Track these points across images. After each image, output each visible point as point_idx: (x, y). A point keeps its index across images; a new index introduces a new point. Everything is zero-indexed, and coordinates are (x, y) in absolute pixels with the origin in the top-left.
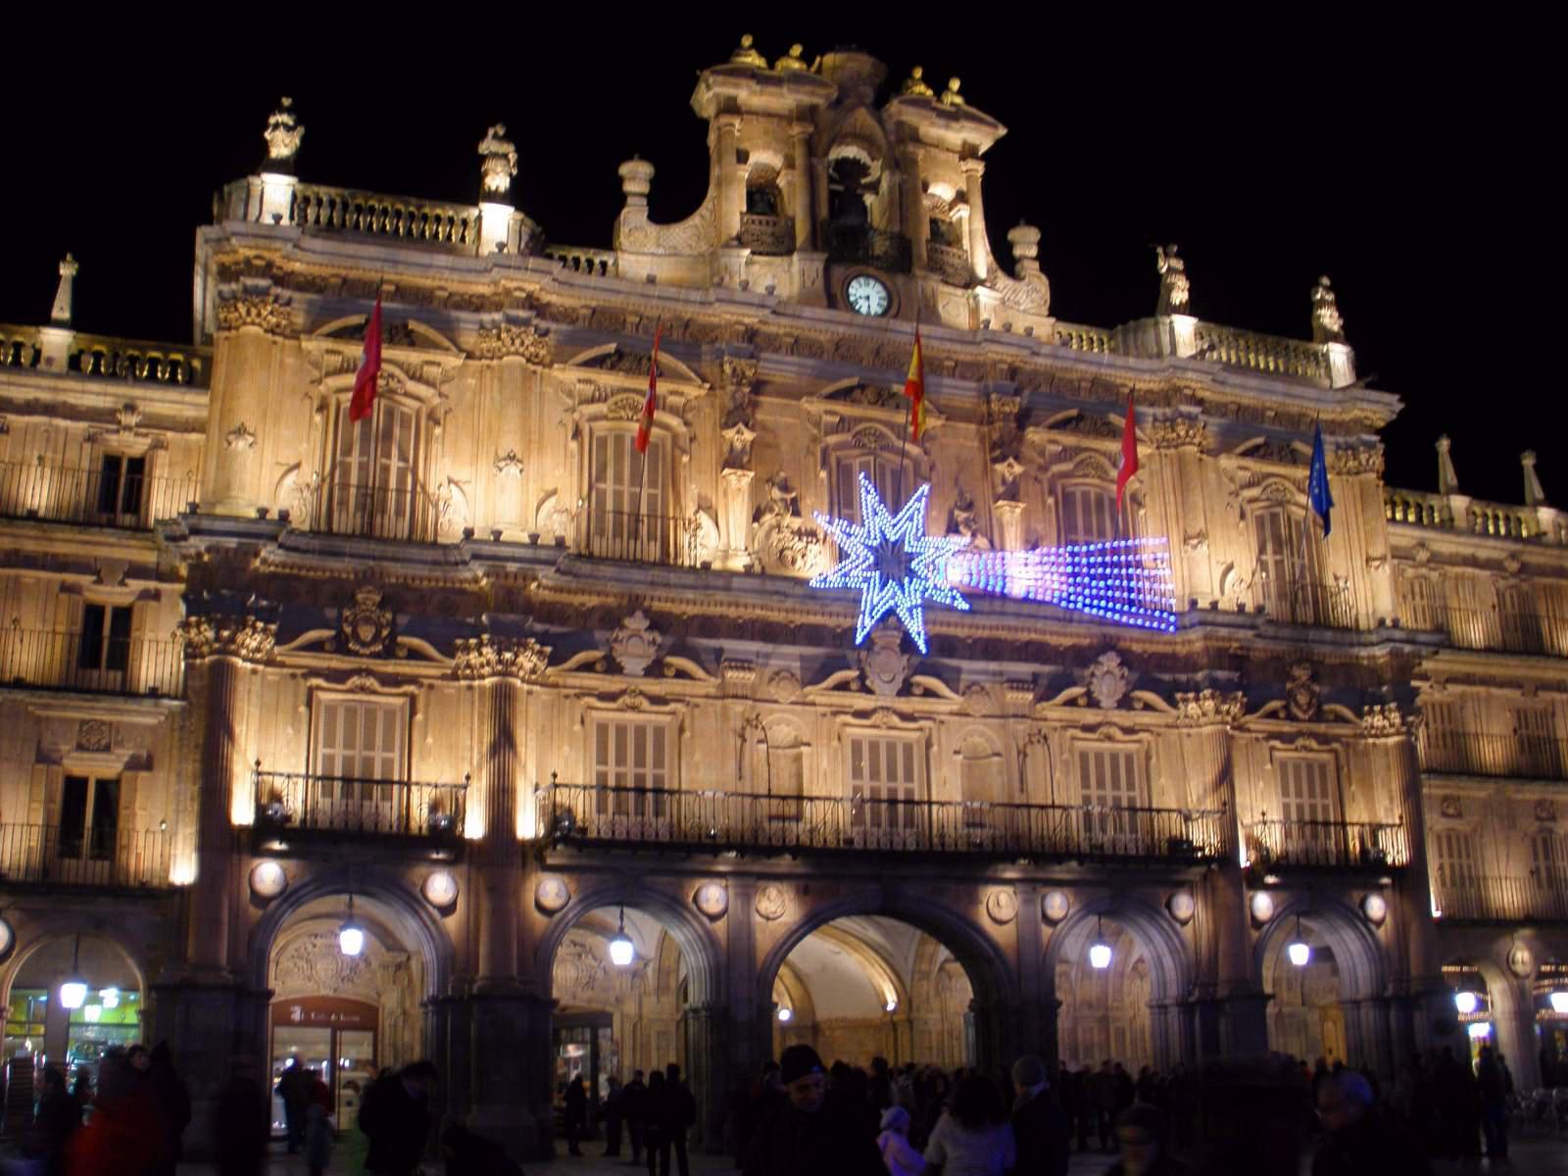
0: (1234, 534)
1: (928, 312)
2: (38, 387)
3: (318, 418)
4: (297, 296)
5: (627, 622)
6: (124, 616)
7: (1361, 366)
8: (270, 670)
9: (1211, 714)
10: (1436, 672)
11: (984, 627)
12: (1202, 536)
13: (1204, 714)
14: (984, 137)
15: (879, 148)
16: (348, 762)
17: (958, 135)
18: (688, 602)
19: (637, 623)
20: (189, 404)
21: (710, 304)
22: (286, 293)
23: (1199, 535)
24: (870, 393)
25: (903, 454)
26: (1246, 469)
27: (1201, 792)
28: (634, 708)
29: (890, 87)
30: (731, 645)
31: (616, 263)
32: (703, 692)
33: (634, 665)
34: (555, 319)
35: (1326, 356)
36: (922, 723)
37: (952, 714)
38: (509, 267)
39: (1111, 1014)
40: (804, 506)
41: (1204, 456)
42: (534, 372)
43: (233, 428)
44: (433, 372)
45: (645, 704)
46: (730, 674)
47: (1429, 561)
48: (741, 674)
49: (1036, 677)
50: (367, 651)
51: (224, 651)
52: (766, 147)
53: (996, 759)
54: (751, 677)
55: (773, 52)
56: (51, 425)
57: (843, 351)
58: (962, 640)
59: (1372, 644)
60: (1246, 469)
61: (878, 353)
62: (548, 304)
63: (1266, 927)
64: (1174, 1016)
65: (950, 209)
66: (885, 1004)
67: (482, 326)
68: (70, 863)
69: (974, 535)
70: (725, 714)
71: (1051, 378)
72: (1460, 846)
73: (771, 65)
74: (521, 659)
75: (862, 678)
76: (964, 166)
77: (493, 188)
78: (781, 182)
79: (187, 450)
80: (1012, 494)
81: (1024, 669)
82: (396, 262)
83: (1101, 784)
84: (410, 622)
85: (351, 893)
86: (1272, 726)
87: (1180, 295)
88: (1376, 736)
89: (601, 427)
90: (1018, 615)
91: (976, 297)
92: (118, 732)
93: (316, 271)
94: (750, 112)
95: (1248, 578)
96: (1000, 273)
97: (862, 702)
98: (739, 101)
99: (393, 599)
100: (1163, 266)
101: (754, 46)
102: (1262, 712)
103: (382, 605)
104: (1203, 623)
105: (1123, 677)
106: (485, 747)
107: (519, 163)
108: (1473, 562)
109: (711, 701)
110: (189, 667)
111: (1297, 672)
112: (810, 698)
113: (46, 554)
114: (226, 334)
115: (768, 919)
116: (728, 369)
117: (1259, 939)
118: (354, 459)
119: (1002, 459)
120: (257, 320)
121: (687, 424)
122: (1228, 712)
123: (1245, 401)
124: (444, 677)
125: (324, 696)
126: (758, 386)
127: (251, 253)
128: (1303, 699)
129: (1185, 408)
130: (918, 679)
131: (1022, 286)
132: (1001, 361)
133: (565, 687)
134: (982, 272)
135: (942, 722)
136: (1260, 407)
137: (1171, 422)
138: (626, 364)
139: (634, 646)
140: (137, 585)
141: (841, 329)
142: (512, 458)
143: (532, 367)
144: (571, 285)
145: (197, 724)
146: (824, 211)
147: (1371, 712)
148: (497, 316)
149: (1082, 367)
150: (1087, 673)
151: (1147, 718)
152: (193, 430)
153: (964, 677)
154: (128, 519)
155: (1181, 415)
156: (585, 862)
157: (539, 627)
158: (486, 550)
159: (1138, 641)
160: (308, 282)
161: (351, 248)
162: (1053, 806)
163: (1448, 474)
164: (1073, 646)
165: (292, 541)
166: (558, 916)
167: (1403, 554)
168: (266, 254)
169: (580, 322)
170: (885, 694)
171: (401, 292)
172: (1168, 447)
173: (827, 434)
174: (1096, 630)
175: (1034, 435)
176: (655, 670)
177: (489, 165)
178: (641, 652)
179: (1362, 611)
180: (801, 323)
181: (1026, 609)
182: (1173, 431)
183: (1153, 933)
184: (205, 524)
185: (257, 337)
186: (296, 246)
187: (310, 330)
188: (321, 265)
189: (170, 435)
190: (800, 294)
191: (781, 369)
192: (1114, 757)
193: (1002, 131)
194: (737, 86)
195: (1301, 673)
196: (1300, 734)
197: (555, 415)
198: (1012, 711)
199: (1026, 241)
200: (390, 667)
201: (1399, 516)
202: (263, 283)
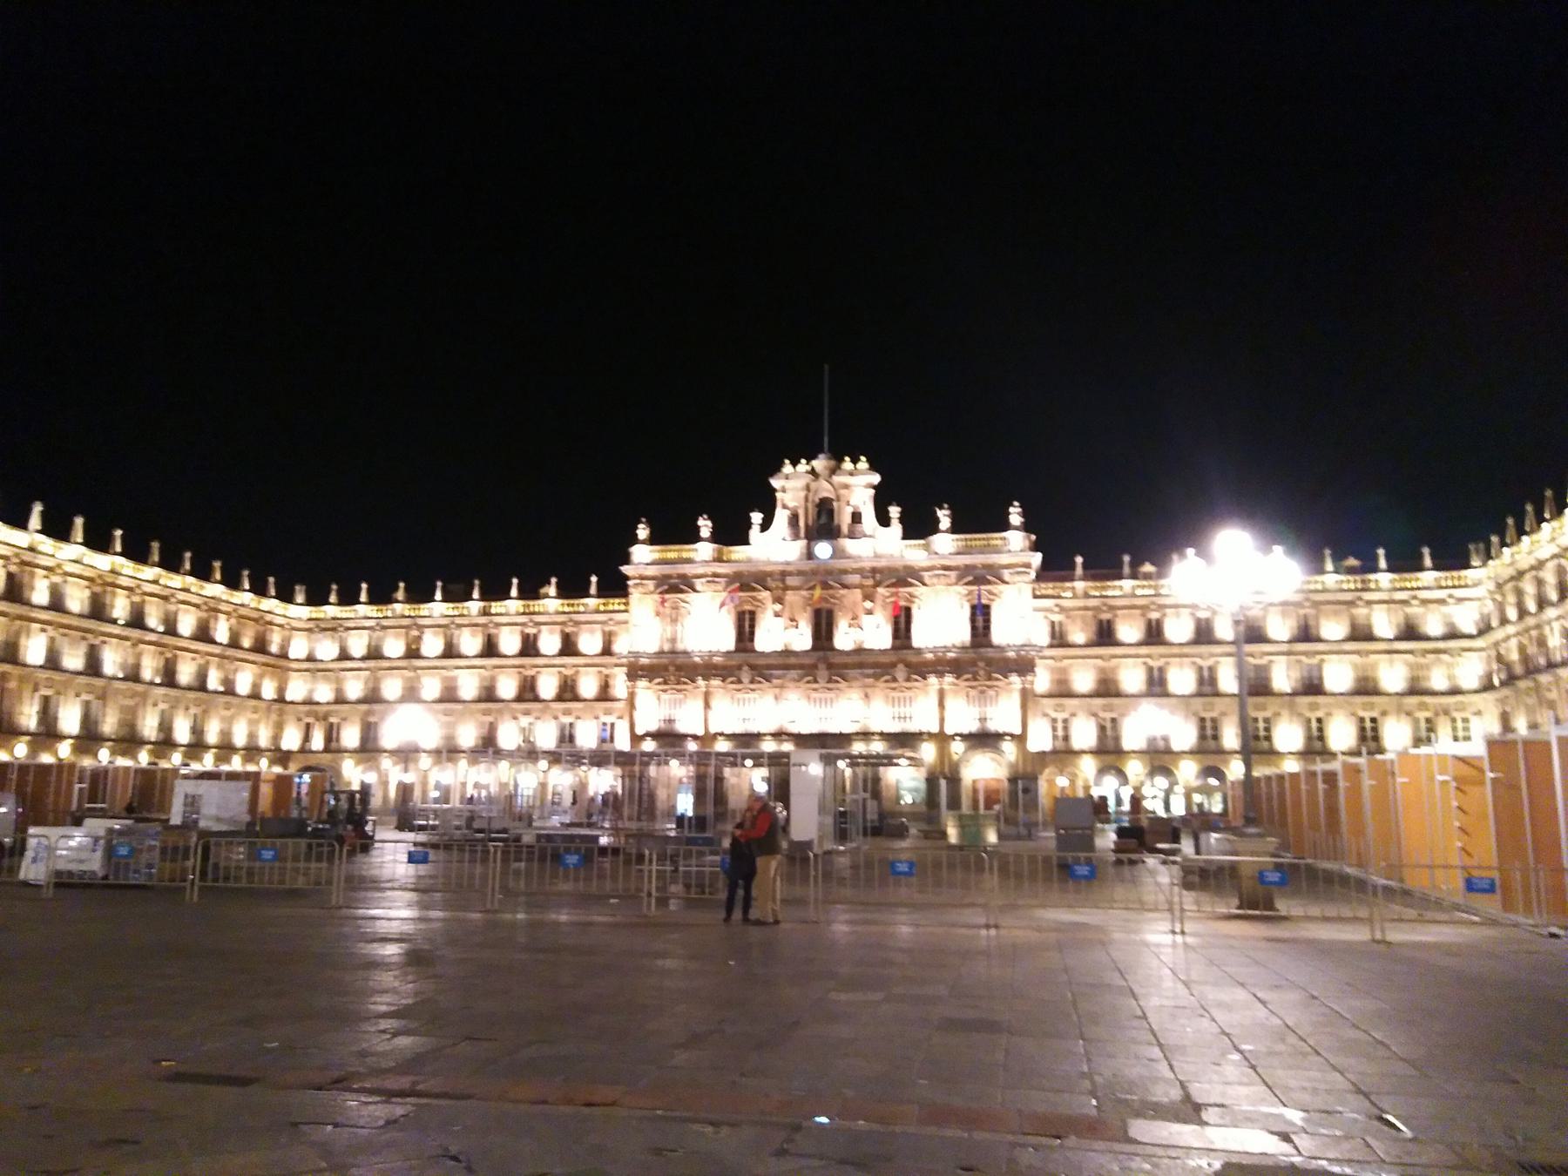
29: (834, 471)
30: (774, 672)
33: (746, 680)
44: (687, 599)
54: (778, 681)
55: (795, 463)
57: (814, 573)
80: (870, 612)
81: (870, 671)
86: (967, 683)
97: (815, 686)
99: (679, 668)
108: (1086, 608)
126: (786, 588)
128: (982, 673)
145: (628, 708)
151: (916, 684)
163: (1079, 571)
170: (822, 683)
175: (881, 590)
187: (652, 593)
195: (981, 664)
196: (981, 685)
199: (894, 511)
200: (678, 687)
202: (638, 581)
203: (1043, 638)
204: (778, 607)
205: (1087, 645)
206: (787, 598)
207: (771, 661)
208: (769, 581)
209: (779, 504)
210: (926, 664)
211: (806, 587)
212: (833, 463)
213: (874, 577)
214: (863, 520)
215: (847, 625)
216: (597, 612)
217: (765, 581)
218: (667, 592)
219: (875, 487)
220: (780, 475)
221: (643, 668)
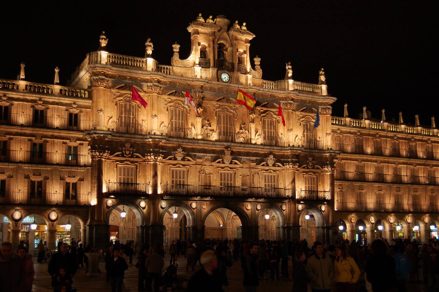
1: (238, 81)
2: (55, 99)
3: (116, 107)
4: (110, 79)
5: (178, 150)
6: (76, 148)
7: (329, 90)
9: (291, 168)
12: (291, 130)
13: (290, 168)
14: (250, 38)
15: (228, 42)
16: (124, 179)
19: (180, 150)
20: (87, 103)
21: (194, 81)
22: (108, 79)
24: (225, 100)
25: (231, 112)
26: (302, 114)
27: (289, 184)
28: (179, 167)
29: (230, 26)
30: (197, 154)
31: (173, 68)
32: (192, 164)
33: (179, 158)
34: (162, 84)
35: (321, 87)
36: (234, 169)
37: (240, 168)
38: (154, 74)
39: (267, 228)
40: (212, 124)
41: (293, 112)
42: (159, 96)
45: (181, 166)
47: (340, 133)
48: (200, 160)
52: (204, 42)
53: (248, 177)
54: (202, 160)
55: (205, 18)
56: (58, 107)
59: (326, 153)
60: (302, 114)
64: (281, 230)
65: (242, 55)
66: (220, 225)
67: (148, 86)
69: (245, 130)
70: (196, 168)
71: (262, 95)
72: (342, 194)
73: (205, 21)
75: (223, 160)
76: (246, 45)
77: (149, 54)
78: (207, 49)
79: (87, 113)
80: (253, 121)
81: (254, 158)
82: (130, 72)
83: (268, 182)
84: (136, 150)
85: (124, 205)
87: (290, 75)
88: (326, 172)
90: (254, 148)
92: (76, 173)
93: (113, 74)
95: (300, 138)
96: (252, 70)
97: (223, 165)
98: (199, 30)
100: (287, 68)
103: (130, 147)
104: (290, 149)
105: (274, 160)
106: (152, 176)
108: (350, 133)
111: (310, 159)
112: (212, 165)
113: (59, 135)
114: (96, 88)
115: (204, 209)
116: (197, 95)
117: (299, 214)
118: (123, 115)
119: (251, 114)
120: (103, 86)
121: (189, 107)
122: (295, 168)
124: (142, 161)
125: (119, 165)
126: (203, 98)
127: (101, 70)
128: (310, 164)
129: (290, 102)
131: (256, 72)
132: (252, 92)
134: (248, 70)
135: (238, 169)
137: (286, 104)
138: (177, 94)
140: (78, 142)
142: (155, 116)
143: (158, 95)
144: (166, 77)
146: (216, 58)
147: (325, 167)
148: (151, 84)
149: (269, 93)
150: (266, 159)
152: (88, 108)
154: (75, 128)
155: (289, 103)
156: (172, 198)
157: (161, 151)
158: (153, 136)
159: (277, 152)
160: (112, 76)
161: (121, 69)
162: (260, 188)
163: (346, 112)
166: (165, 209)
168: (104, 71)
169: (167, 85)
170: (227, 163)
171: (131, 78)
172: (285, 110)
173: (216, 109)
174: (269, 150)
176: (183, 159)
178: (181, 156)
179: (324, 145)
180: (212, 85)
181: (255, 146)
182: (287, 106)
183: (278, 213)
185: (103, 89)
186: (110, 69)
187: (113, 87)
188: (115, 72)
189: (83, 109)
190: (212, 78)
191: (207, 94)
192: (271, 176)
193: (254, 36)
196: (310, 172)
197: (162, 105)
199: (257, 61)
200: (132, 159)
201: (334, 123)
202: (104, 77)
204: (200, 110)
205: (351, 153)
207: (196, 146)
210: (283, 156)
211: (217, 99)
218: (121, 88)
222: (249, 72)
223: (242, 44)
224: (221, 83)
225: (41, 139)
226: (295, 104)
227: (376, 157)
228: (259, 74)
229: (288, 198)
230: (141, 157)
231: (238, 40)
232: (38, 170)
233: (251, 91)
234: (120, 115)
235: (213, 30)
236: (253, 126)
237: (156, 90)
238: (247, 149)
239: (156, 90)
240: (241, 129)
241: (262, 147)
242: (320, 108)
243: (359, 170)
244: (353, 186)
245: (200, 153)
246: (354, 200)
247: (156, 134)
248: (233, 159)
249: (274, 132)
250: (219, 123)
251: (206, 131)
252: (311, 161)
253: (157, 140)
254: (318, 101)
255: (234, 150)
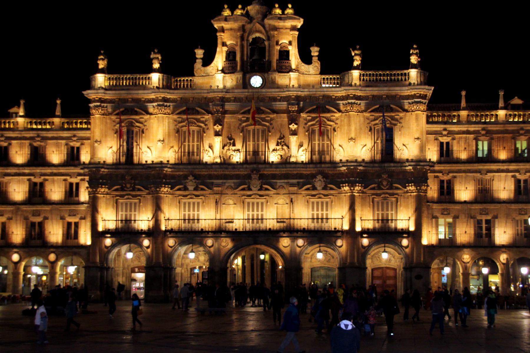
0: (367, 136)
3: (115, 135)
4: (108, 105)
5: (189, 178)
8: (108, 196)
10: (446, 170)
11: (283, 171)
12: (351, 139)
16: (126, 215)
17: (289, 24)
18: (204, 171)
19: (191, 178)
22: (105, 105)
23: (351, 139)
28: (191, 198)
30: (215, 181)
32: (209, 193)
33: (191, 188)
37: (274, 194)
43: (95, 140)
44: (141, 120)
45: (194, 197)
46: (215, 188)
47: (448, 134)
48: (217, 188)
49: (298, 182)
50: (128, 190)
51: (94, 193)
52: (231, 40)
54: (220, 189)
55: (232, 10)
57: (248, 100)
58: (278, 174)
61: (258, 98)
62: (170, 98)
63: (366, 248)
67: (154, 107)
68: (69, 241)
69: (282, 146)
73: (232, 13)
74: (162, 190)
76: (292, 32)
80: (294, 133)
81: (295, 181)
82: (130, 94)
86: (372, 192)
88: (412, 193)
89: (185, 129)
90: (290, 168)
91: (290, 75)
93: (112, 98)
94: (227, 30)
96: (303, 64)
97: (249, 193)
99: (134, 177)
101: (228, 8)
102: (369, 188)
103: (131, 179)
107: (161, 60)
108: (468, 132)
109: (211, 195)
110: (89, 197)
111: (383, 176)
112: (236, 193)
113: (59, 172)
119: (290, 124)
121: (206, 125)
123: (375, 94)
124: (146, 194)
125: (121, 201)
126: (225, 112)
127: (95, 97)
129: (350, 101)
130: (264, 186)
131: (311, 66)
133: (175, 194)
134: (293, 67)
135: (271, 196)
136: (381, 94)
138: (189, 112)
139: (190, 183)
140: (80, 178)
141: (247, 94)
142: (159, 141)
145: (90, 209)
147: (409, 186)
148: (156, 104)
150: (314, 180)
151: (332, 192)
153: (278, 184)
154: (76, 162)
155: (349, 103)
157: (168, 181)
163: (463, 104)
164: (311, 174)
165: (108, 167)
167: (439, 133)
169: (178, 102)
172: (346, 112)
173: (243, 123)
174: (316, 169)
175: (303, 115)
177: (154, 61)
181: (293, 166)
184: (86, 166)
185: (100, 118)
189: (85, 141)
194: (220, 23)
196: (384, 193)
197: (172, 127)
198: (291, 192)
199: (315, 51)
200: (134, 193)
202: (98, 104)
203: (433, 155)
204: (218, 128)
206: (226, 120)
208: (212, 107)
209: (219, 42)
212: (264, 9)
213: (298, 104)
214: (290, 57)
215: (275, 143)
216: (62, 129)
217: (209, 106)
219: (298, 30)
220: (220, 17)
221: (103, 177)
222: (294, 69)
223: (286, 33)
224: (250, 90)
225: (40, 178)
226: (363, 103)
227: (514, 164)
228: (316, 68)
229: (336, 231)
230: (143, 189)
231: (279, 29)
232: (37, 210)
233: (291, 95)
234: (121, 144)
235: (241, 24)
236: (293, 140)
237: (160, 111)
238: (283, 170)
239: (160, 111)
240: (277, 145)
241: (302, 166)
242: (406, 102)
243: (482, 185)
244: (471, 209)
245: (218, 179)
246: (471, 231)
247: (154, 162)
248: (262, 184)
249: (327, 144)
250: (245, 141)
251: (228, 152)
252: (385, 179)
253: (157, 169)
254: (402, 94)
255: (266, 173)
